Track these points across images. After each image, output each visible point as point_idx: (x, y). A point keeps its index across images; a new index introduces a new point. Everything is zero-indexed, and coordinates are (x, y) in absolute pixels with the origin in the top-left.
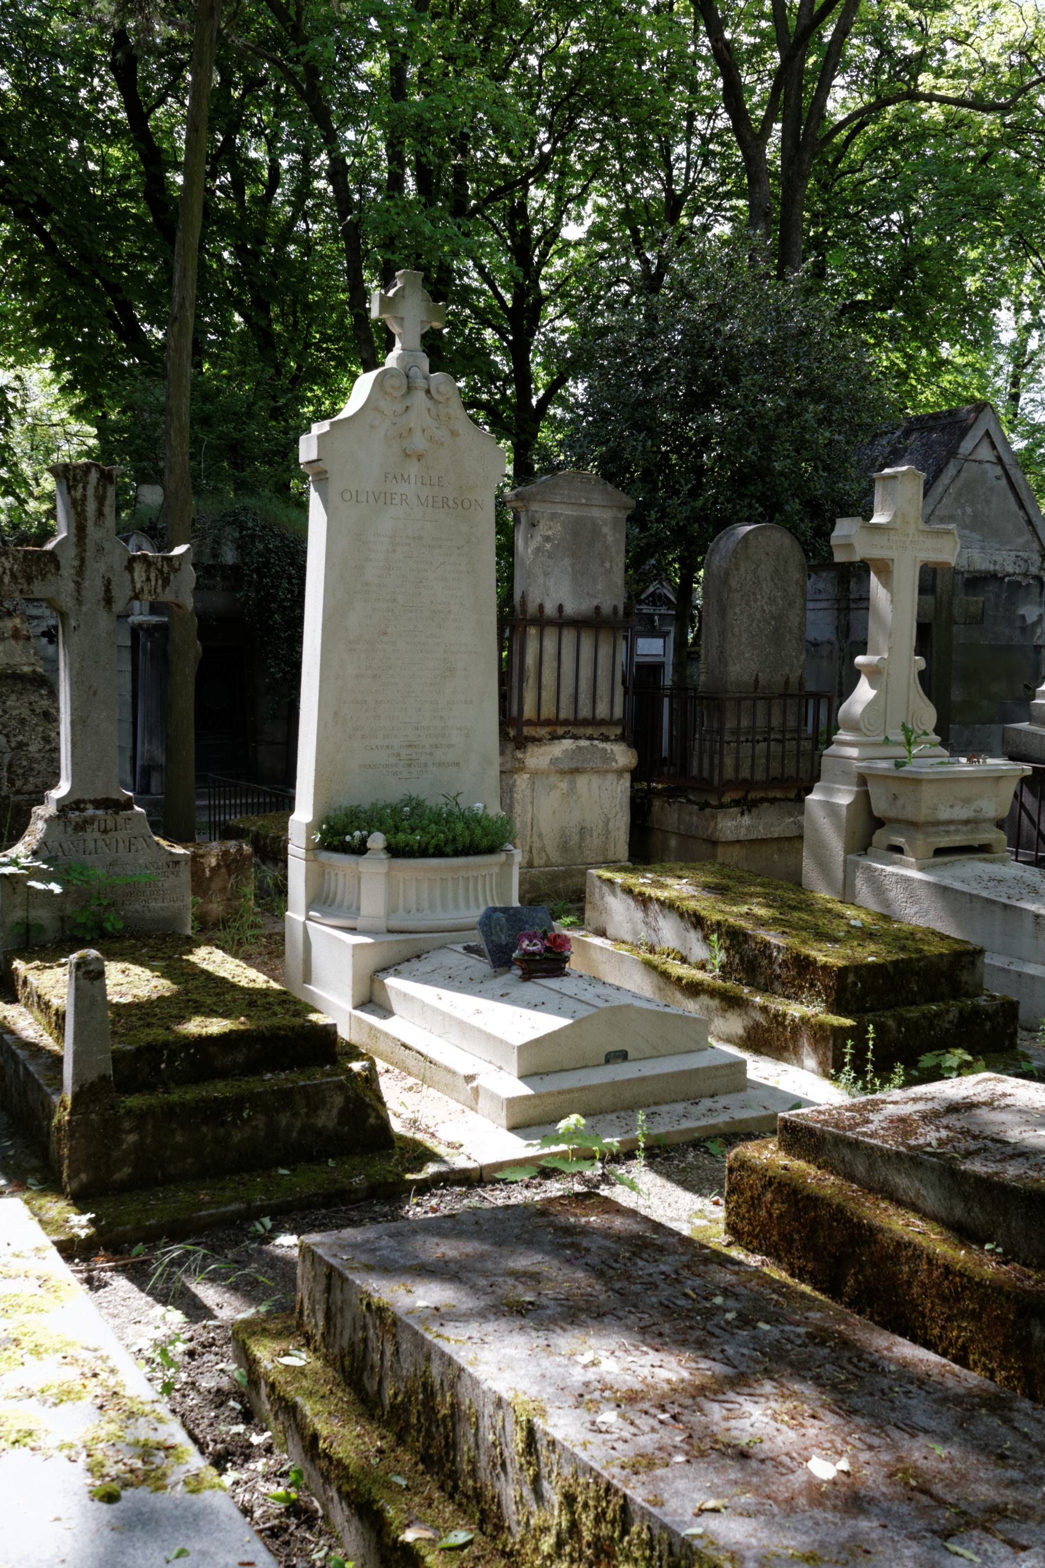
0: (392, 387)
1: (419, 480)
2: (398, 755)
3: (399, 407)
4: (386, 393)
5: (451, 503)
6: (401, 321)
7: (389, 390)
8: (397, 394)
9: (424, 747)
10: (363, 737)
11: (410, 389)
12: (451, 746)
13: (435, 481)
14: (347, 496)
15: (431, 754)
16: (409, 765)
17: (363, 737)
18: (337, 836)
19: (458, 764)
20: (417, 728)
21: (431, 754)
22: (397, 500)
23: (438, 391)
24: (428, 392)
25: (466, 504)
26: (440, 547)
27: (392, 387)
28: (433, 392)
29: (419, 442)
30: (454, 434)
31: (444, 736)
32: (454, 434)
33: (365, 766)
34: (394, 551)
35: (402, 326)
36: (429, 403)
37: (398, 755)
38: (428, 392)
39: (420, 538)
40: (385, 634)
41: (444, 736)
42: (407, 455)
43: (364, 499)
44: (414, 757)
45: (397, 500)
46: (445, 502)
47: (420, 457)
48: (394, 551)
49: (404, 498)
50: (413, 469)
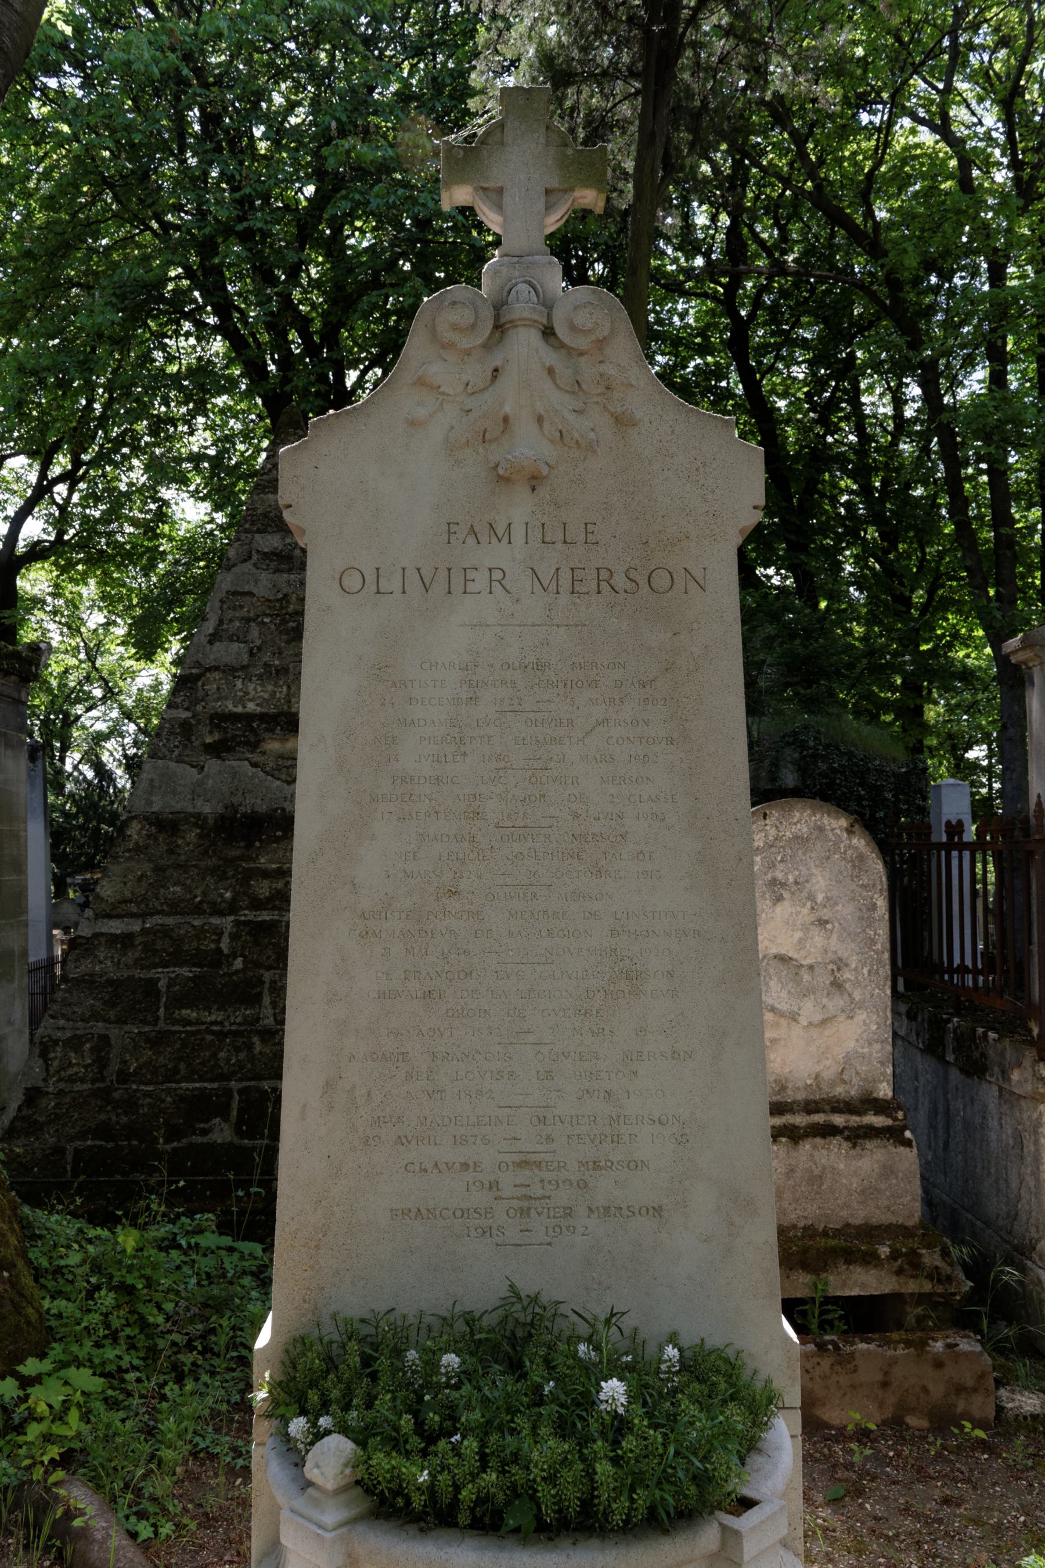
0: (455, 327)
1: (536, 534)
2: (494, 1185)
3: (476, 372)
4: (444, 347)
5: (620, 581)
6: (496, 196)
7: (449, 336)
8: (465, 343)
9: (561, 1167)
10: (400, 1140)
11: (500, 328)
12: (637, 1165)
13: (576, 532)
14: (353, 582)
15: (583, 1185)
16: (524, 1212)
17: (400, 1140)
18: (297, 1393)
19: (658, 1210)
20: (543, 1120)
21: (583, 1185)
22: (480, 580)
23: (573, 328)
24: (548, 332)
25: (661, 580)
26: (594, 684)
27: (455, 327)
28: (561, 330)
29: (528, 446)
30: (623, 421)
31: (616, 1140)
32: (623, 421)
33: (405, 1213)
34: (474, 700)
35: (499, 207)
36: (550, 356)
37: (494, 1185)
38: (548, 332)
39: (540, 666)
40: (453, 893)
41: (616, 1140)
42: (504, 480)
43: (396, 585)
44: (537, 1191)
45: (480, 580)
46: (604, 578)
47: (535, 482)
48: (474, 700)
49: (497, 578)
50: (519, 509)
